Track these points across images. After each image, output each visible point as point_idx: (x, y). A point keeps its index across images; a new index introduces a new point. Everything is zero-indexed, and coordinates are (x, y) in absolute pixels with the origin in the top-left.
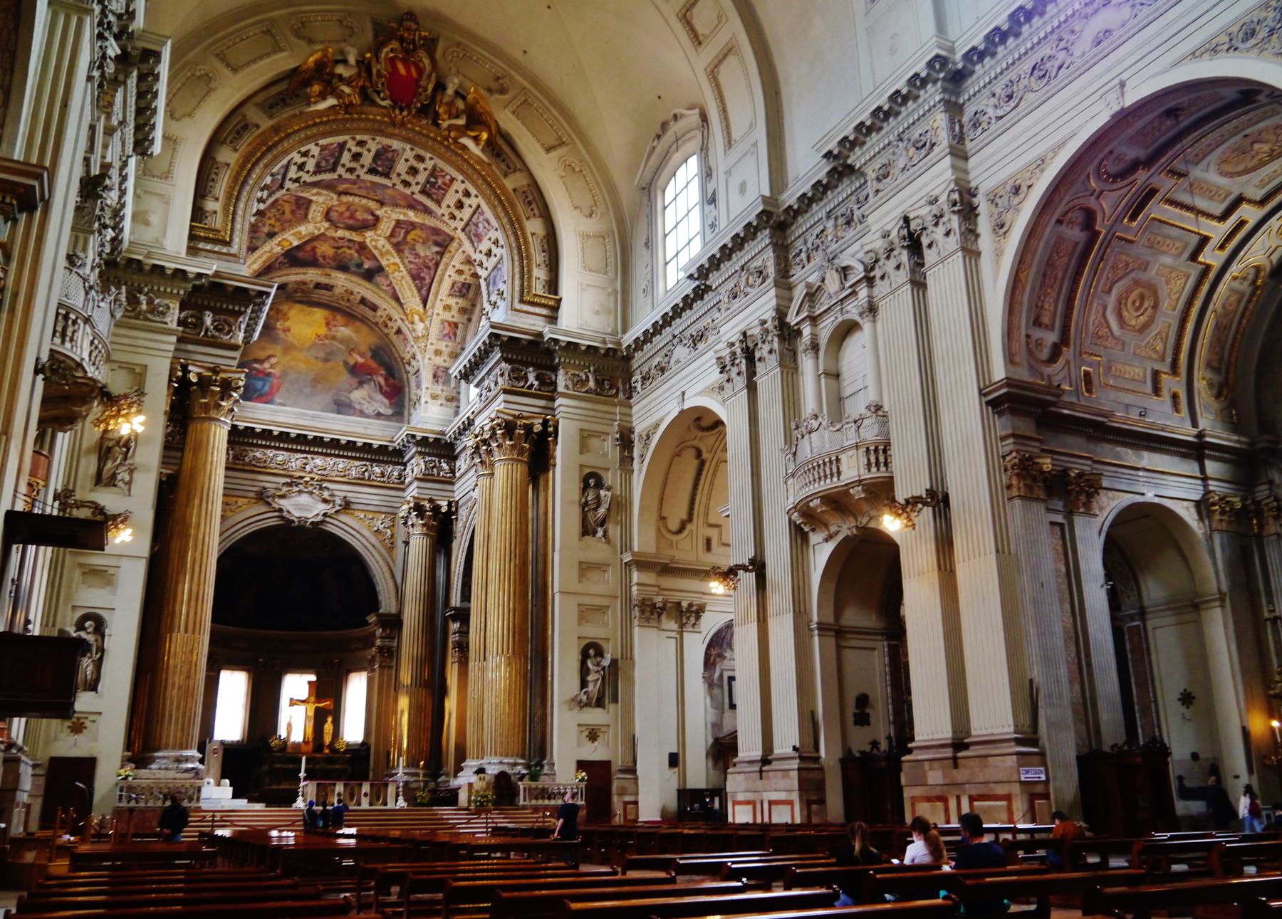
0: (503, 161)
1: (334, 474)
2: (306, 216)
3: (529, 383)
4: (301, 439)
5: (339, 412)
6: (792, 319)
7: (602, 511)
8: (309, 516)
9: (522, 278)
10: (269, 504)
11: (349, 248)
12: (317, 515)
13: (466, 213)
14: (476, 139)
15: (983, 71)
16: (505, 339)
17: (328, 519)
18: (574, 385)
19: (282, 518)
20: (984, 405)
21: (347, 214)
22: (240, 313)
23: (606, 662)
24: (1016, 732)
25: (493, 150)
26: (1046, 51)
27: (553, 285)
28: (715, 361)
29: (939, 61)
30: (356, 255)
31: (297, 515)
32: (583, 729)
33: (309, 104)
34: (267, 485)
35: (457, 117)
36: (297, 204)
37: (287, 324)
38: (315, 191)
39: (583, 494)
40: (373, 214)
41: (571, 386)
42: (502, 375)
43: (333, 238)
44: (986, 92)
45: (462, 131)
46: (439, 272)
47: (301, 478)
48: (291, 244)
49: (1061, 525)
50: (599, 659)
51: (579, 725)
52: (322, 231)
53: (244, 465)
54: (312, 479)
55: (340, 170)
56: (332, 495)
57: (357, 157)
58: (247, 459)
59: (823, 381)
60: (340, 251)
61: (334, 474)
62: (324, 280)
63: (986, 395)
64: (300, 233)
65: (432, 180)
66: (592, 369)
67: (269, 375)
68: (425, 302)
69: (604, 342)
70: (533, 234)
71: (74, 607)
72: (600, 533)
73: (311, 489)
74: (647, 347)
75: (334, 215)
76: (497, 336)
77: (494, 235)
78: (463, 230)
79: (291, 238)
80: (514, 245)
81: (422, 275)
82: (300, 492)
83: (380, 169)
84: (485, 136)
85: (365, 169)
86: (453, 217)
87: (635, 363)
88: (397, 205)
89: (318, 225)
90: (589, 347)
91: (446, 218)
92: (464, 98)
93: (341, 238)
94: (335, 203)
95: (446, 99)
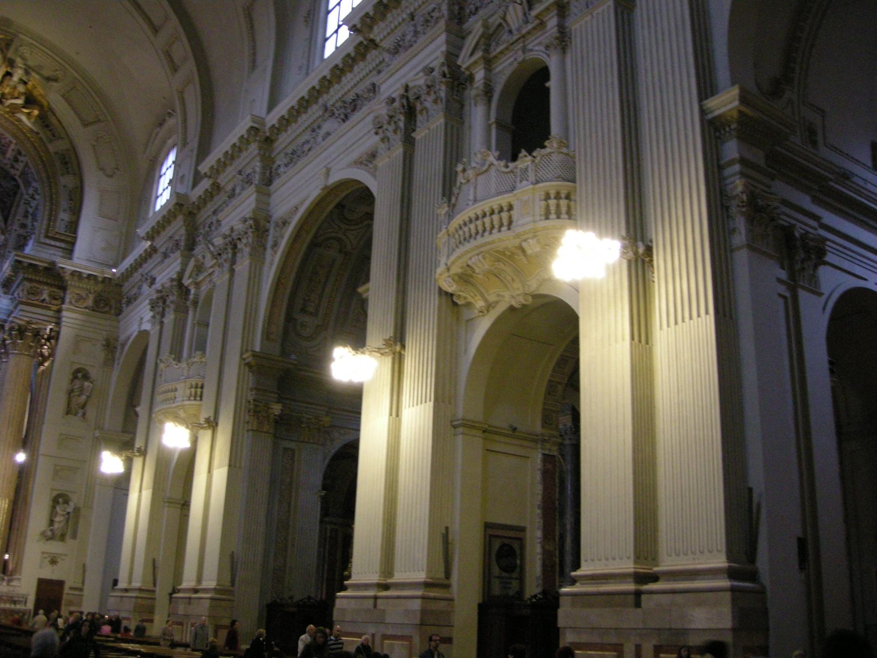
0: (50, 130)
3: (42, 298)
6: (186, 282)
7: (84, 397)
9: (49, 220)
13: (20, 166)
14: (29, 114)
15: (283, 141)
16: (26, 265)
18: (76, 301)
20: (242, 368)
23: (70, 509)
24: (218, 585)
25: (44, 122)
26: (307, 136)
27: (73, 227)
28: (147, 301)
29: (254, 130)
35: (17, 98)
39: (71, 383)
41: (73, 301)
42: (23, 290)
44: (282, 155)
46: (17, 199)
49: (293, 451)
50: (66, 506)
51: (43, 553)
59: (196, 328)
63: (244, 359)
68: (6, 220)
70: (65, 186)
72: (80, 414)
74: (131, 280)
76: (19, 262)
77: (34, 184)
81: (5, 200)
84: (36, 112)
86: (13, 167)
87: (125, 289)
90: (90, 275)
91: (9, 166)
92: (25, 83)
95: (12, 83)
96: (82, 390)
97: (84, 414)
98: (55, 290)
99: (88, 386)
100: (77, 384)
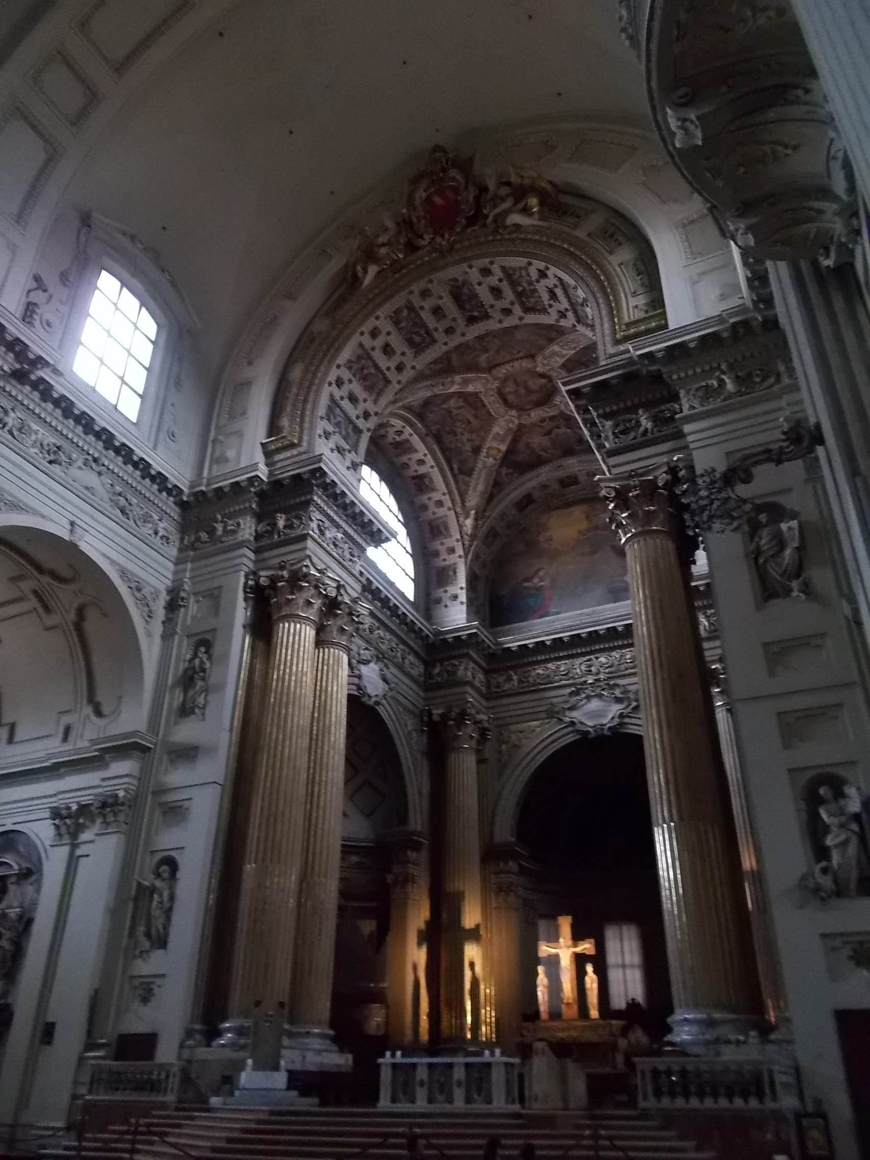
1: (622, 667)
2: (491, 415)
3: (642, 429)
4: (576, 640)
5: (616, 600)
8: (605, 722)
10: (561, 720)
11: (558, 427)
12: (613, 718)
17: (627, 720)
18: (705, 399)
19: (578, 731)
21: (522, 391)
22: (309, 502)
30: (568, 430)
31: (591, 724)
32: (838, 942)
33: (362, 284)
34: (555, 700)
36: (470, 405)
37: (549, 533)
38: (458, 378)
40: (542, 376)
43: (534, 425)
45: (507, 213)
47: (585, 682)
48: (499, 450)
51: (823, 936)
52: (516, 422)
53: (529, 686)
54: (598, 680)
55: (440, 336)
56: (626, 692)
57: (437, 311)
58: (531, 679)
60: (553, 435)
61: (622, 667)
62: (561, 474)
64: (498, 434)
65: (520, 289)
66: (723, 367)
67: (539, 589)
69: (720, 319)
71: (152, 852)
73: (598, 690)
75: (511, 398)
78: (579, 322)
79: (495, 444)
80: (596, 289)
82: (588, 698)
83: (476, 314)
85: (461, 322)
88: (541, 348)
89: (507, 417)
93: (543, 421)
94: (497, 384)
96: (780, 542)
97: (807, 589)
98: (663, 408)
99: (790, 528)
100: (765, 539)
